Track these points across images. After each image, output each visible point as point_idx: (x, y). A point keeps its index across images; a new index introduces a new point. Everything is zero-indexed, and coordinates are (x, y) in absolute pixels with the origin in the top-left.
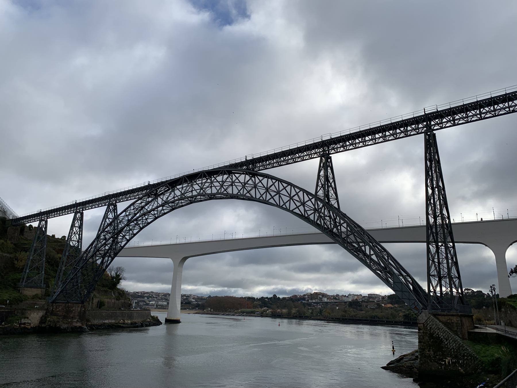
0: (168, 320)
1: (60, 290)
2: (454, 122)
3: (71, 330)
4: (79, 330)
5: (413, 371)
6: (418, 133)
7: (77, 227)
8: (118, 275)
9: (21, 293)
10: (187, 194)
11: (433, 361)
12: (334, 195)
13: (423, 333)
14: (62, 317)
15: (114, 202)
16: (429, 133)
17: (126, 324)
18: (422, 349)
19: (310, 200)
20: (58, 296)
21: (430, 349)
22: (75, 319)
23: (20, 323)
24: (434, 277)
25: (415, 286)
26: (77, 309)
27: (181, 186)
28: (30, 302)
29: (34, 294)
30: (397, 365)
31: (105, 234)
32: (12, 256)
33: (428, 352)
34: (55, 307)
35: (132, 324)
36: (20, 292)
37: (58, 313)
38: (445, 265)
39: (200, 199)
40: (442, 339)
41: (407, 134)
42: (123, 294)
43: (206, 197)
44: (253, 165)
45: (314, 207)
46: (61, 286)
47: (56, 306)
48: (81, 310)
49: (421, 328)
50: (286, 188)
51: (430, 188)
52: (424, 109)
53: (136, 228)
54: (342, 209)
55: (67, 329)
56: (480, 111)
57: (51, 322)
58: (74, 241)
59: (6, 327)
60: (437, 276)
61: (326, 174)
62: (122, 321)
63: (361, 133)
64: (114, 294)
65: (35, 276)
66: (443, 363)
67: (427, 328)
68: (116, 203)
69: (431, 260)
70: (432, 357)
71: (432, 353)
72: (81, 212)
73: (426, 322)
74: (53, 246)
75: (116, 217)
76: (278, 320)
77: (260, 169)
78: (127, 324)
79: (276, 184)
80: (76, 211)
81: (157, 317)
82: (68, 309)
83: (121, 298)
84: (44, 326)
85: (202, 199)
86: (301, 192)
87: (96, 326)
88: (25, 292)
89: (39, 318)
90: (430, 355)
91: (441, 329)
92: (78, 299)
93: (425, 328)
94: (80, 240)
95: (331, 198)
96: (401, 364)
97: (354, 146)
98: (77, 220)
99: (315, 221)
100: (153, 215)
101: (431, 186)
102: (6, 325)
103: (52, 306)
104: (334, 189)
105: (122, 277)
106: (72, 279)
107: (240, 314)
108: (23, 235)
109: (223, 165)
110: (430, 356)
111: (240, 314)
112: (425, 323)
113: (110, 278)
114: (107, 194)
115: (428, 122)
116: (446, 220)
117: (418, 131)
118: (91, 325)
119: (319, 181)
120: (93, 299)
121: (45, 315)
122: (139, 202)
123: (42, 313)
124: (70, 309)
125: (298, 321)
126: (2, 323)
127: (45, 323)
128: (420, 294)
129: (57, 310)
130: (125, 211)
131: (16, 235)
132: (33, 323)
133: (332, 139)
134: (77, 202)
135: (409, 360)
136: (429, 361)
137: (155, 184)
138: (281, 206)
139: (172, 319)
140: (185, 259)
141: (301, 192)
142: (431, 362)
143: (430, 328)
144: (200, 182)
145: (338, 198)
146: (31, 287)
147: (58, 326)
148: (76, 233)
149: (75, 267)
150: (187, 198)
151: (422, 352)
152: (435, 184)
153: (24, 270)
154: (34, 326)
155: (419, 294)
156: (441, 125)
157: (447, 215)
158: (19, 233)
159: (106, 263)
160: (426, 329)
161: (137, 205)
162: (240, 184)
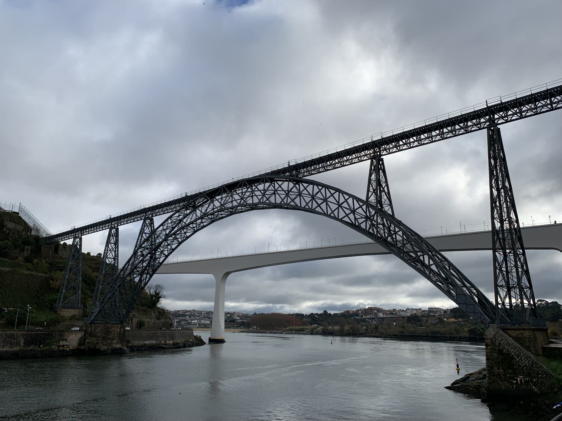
0: (211, 339)
1: (98, 310)
2: (521, 115)
5: (481, 391)
6: (480, 129)
7: (113, 243)
9: (58, 314)
10: (227, 205)
11: (502, 379)
12: (387, 200)
13: (491, 349)
14: (102, 338)
15: (151, 216)
16: (492, 128)
17: (167, 345)
18: (490, 367)
19: (361, 207)
20: (96, 316)
21: (499, 366)
22: (115, 340)
23: (58, 345)
24: (502, 288)
25: (481, 298)
26: (116, 329)
27: (220, 197)
28: (68, 323)
29: (71, 315)
30: (463, 384)
31: (142, 250)
34: (93, 328)
35: (173, 344)
36: (57, 313)
38: (515, 274)
39: (241, 210)
40: (513, 355)
41: (468, 130)
42: (163, 313)
43: (247, 208)
44: (297, 170)
45: (365, 215)
46: (99, 306)
47: (95, 327)
48: (120, 331)
49: (489, 344)
50: (334, 195)
51: (494, 189)
52: (486, 101)
53: (174, 243)
54: (397, 216)
55: (106, 350)
56: (551, 100)
57: (90, 343)
58: (110, 258)
59: (45, 350)
60: (505, 286)
61: (378, 178)
62: (163, 341)
63: (416, 131)
64: (154, 313)
65: (72, 296)
66: (515, 382)
67: (496, 344)
68: (152, 216)
69: (498, 269)
70: (502, 375)
71: (502, 371)
72: (116, 227)
73: (494, 337)
74: (89, 264)
75: (153, 232)
76: (330, 338)
77: (304, 175)
78: (168, 344)
79: (323, 191)
80: (111, 226)
81: (200, 337)
82: (106, 329)
83: (161, 317)
84: (83, 348)
85: (243, 209)
86: (351, 199)
88: (62, 313)
91: (512, 345)
92: (117, 319)
93: (493, 343)
94: (116, 258)
95: (384, 204)
96: (467, 384)
97: (408, 145)
98: (112, 235)
99: (367, 230)
100: (192, 228)
101: (496, 187)
102: (44, 347)
104: (387, 194)
105: (161, 295)
106: (110, 298)
107: (288, 332)
108: (57, 254)
109: (264, 173)
110: (499, 374)
111: (288, 332)
112: (493, 339)
113: (149, 297)
114: (142, 208)
115: (492, 116)
116: (514, 224)
117: (479, 126)
119: (370, 186)
120: (132, 319)
122: (177, 215)
123: (80, 335)
124: (109, 329)
125: (351, 338)
126: (41, 345)
128: (487, 307)
129: (96, 331)
130: (162, 225)
131: (51, 254)
132: (71, 345)
133: (383, 139)
134: (112, 217)
135: (476, 379)
136: (498, 380)
137: (192, 195)
138: (329, 214)
139: (216, 338)
140: (228, 274)
141: (351, 199)
142: (501, 381)
143: (499, 344)
144: (240, 191)
145: (392, 204)
146: (68, 308)
147: (98, 347)
148: (112, 249)
149: (113, 286)
150: (227, 209)
151: (490, 370)
152: (501, 185)
153: (60, 290)
154: (73, 348)
155: (486, 307)
156: (506, 118)
157: (515, 218)
158: (53, 252)
159: (144, 281)
160: (494, 345)
161: (175, 218)
162: (283, 193)
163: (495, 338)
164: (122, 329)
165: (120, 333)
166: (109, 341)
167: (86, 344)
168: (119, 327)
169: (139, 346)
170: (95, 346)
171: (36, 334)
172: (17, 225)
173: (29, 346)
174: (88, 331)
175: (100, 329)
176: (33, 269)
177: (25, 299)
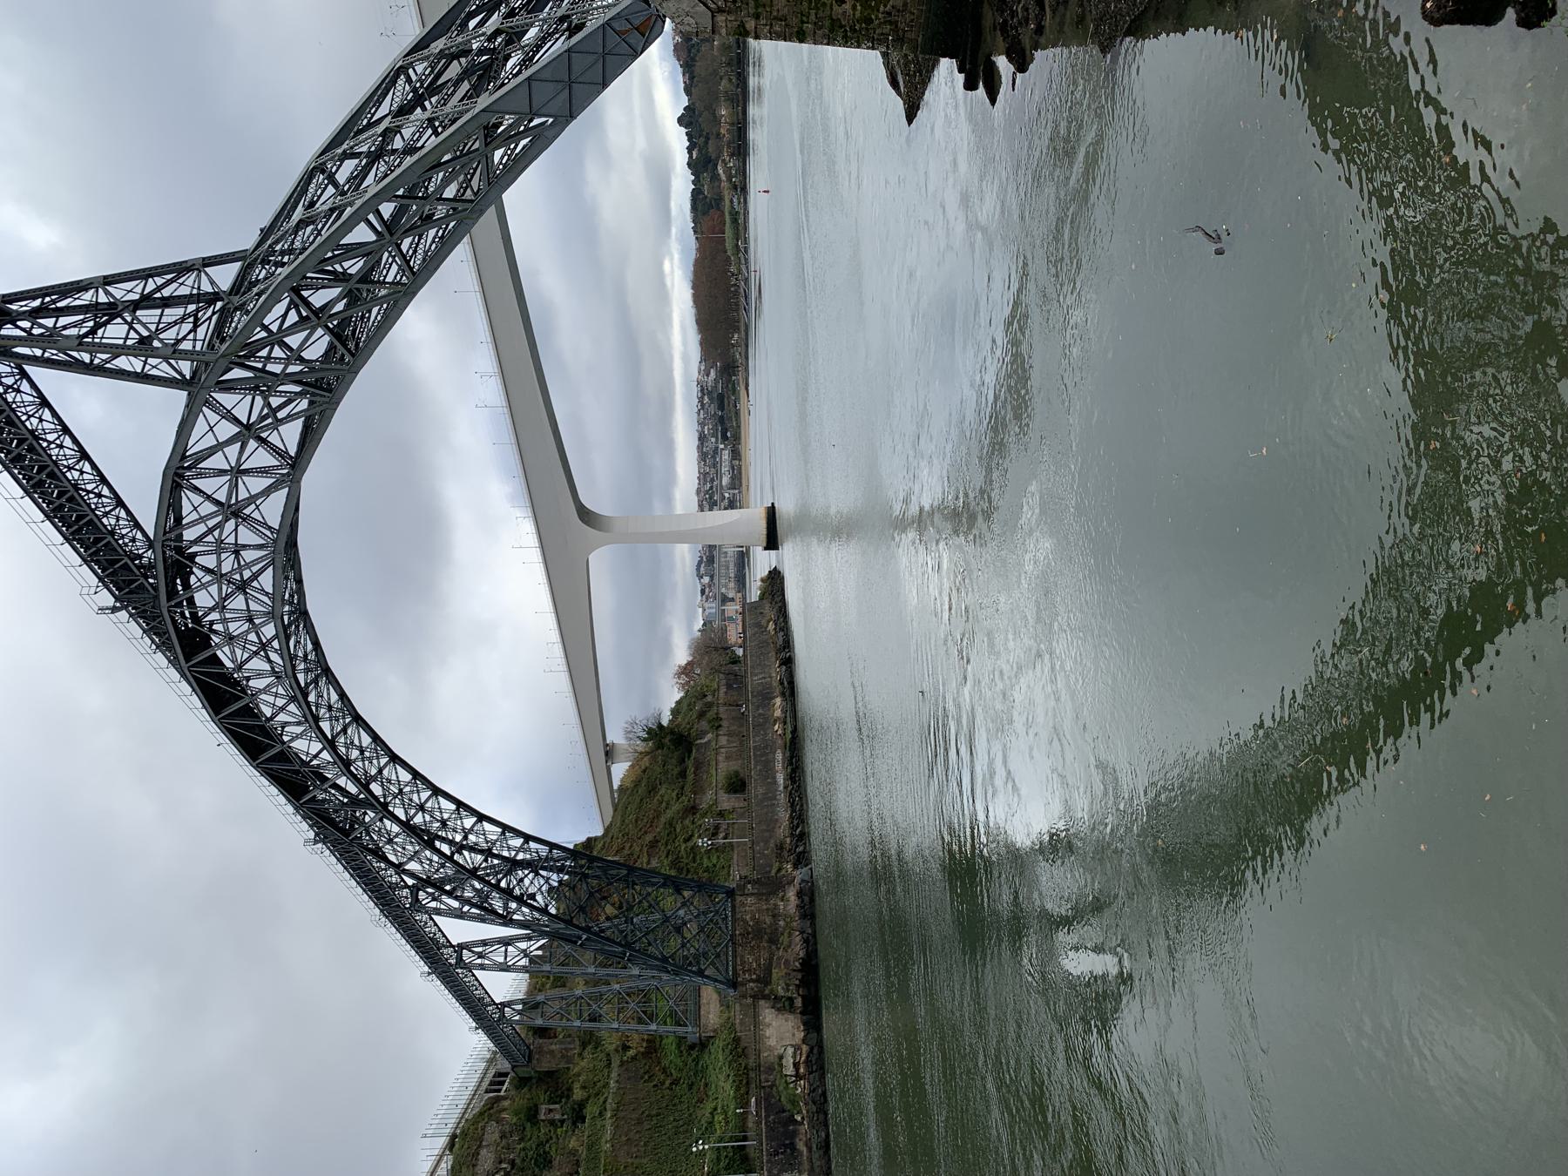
3: (809, 923)
4: (806, 899)
8: (648, 733)
13: (757, 17)
14: (773, 947)
18: (832, 31)
22: (775, 905)
26: (750, 906)
32: (616, 1063)
35: (783, 694)
48: (752, 894)
55: (805, 935)
57: (787, 985)
59: (808, 1112)
64: (704, 733)
76: (756, 136)
78: (784, 711)
81: (762, 580)
82: (750, 936)
84: (800, 1000)
87: (795, 822)
89: (780, 1016)
95: (199, 288)
103: (743, 984)
107: (743, 262)
111: (743, 262)
118: (792, 835)
123: (767, 1011)
125: (751, 69)
127: (791, 1000)
132: (794, 1035)
136: (885, 6)
139: (764, 532)
140: (585, 515)
147: (797, 964)
164: (746, 892)
165: (758, 895)
168: (742, 898)
169: (791, 815)
171: (767, 1140)
172: (484, 1143)
173: (801, 1153)
175: (749, 954)
176: (602, 1099)
177: (681, 1123)
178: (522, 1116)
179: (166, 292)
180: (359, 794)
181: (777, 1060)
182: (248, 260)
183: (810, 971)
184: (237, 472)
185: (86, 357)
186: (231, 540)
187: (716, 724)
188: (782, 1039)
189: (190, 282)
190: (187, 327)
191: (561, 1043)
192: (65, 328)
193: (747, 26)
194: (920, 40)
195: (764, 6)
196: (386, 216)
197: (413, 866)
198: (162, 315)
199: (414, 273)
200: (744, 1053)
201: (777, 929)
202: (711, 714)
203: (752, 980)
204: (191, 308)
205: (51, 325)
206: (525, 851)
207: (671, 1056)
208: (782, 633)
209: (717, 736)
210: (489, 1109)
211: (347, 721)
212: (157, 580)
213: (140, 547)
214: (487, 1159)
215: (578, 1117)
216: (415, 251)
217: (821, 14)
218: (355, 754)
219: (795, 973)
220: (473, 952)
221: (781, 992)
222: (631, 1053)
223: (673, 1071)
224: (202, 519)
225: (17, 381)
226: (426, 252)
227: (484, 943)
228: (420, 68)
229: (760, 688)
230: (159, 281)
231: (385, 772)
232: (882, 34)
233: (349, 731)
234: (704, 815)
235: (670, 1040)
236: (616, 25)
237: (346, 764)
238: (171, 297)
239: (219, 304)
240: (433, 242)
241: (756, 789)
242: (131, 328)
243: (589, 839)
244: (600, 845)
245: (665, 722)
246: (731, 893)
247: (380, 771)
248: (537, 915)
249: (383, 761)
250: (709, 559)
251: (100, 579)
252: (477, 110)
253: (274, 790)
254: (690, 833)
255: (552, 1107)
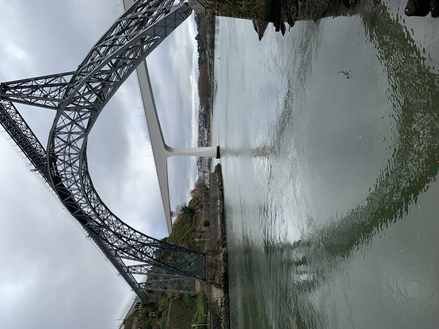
0: (217, 156)
3: (226, 263)
8: (182, 209)
13: (218, 10)
14: (216, 270)
18: (239, 14)
21: (238, 4)
22: (217, 258)
26: (209, 258)
28: (205, 288)
32: (171, 301)
33: (243, 7)
35: (220, 199)
37: (213, 274)
48: (210, 255)
54: (74, 69)
57: (219, 281)
59: (224, 316)
64: (197, 210)
67: (212, 4)
70: (249, 3)
73: (203, 4)
76: (217, 43)
78: (221, 204)
81: (215, 167)
82: (210, 266)
84: (223, 285)
87: (223, 235)
90: (246, 6)
95: (61, 82)
110: (248, 6)
121: (214, 284)
127: (220, 285)
132: (221, 295)
136: (254, 8)
139: (216, 153)
140: (166, 147)
147: (222, 275)
154: (223, 293)
163: (204, 4)
164: (209, 254)
166: (218, 263)
167: (220, 283)
170: (222, 277)
171: (213, 324)
173: (222, 328)
174: (211, 281)
175: (209, 271)
176: (167, 311)
177: (189, 318)
178: (144, 315)
179: (52, 83)
180: (101, 224)
181: (216, 302)
182: (75, 74)
183: (226, 277)
184: (70, 133)
185: (29, 100)
186: (68, 152)
187: (201, 207)
188: (217, 296)
189: (58, 80)
190: (57, 92)
191: (156, 295)
192: (24, 92)
193: (215, 12)
194: (263, 17)
195: (220, 7)
196: (113, 63)
197: (116, 244)
198: (50, 89)
199: (121, 79)
200: (207, 300)
201: (217, 265)
202: (200, 204)
203: (209, 279)
204: (59, 87)
205: (20, 91)
206: (147, 241)
207: (186, 300)
208: (220, 182)
209: (202, 210)
210: (135, 313)
211: (99, 203)
212: (47, 162)
213: (43, 153)
214: (134, 326)
215: (160, 316)
216: (121, 73)
217: (236, 9)
218: (101, 212)
219: (221, 277)
220: (132, 269)
221: (218, 282)
222: (175, 298)
223: (187, 304)
224: (60, 146)
225: (10, 106)
226: (124, 73)
227: (135, 266)
228: (124, 22)
229: (214, 197)
230: (50, 79)
231: (109, 218)
232: (253, 15)
233: (99, 206)
234: (197, 232)
235: (186, 295)
236: (178, 11)
237: (98, 215)
238: (53, 84)
239: (66, 86)
240: (126, 70)
241: (212, 225)
242: (42, 92)
243: (165, 238)
244: (168, 240)
245: (187, 206)
246: (204, 254)
247: (107, 217)
248: (150, 259)
249: (108, 215)
250: (201, 160)
251: (31, 162)
252: (139, 34)
253: (78, 222)
254: (193, 237)
255: (153, 313)
